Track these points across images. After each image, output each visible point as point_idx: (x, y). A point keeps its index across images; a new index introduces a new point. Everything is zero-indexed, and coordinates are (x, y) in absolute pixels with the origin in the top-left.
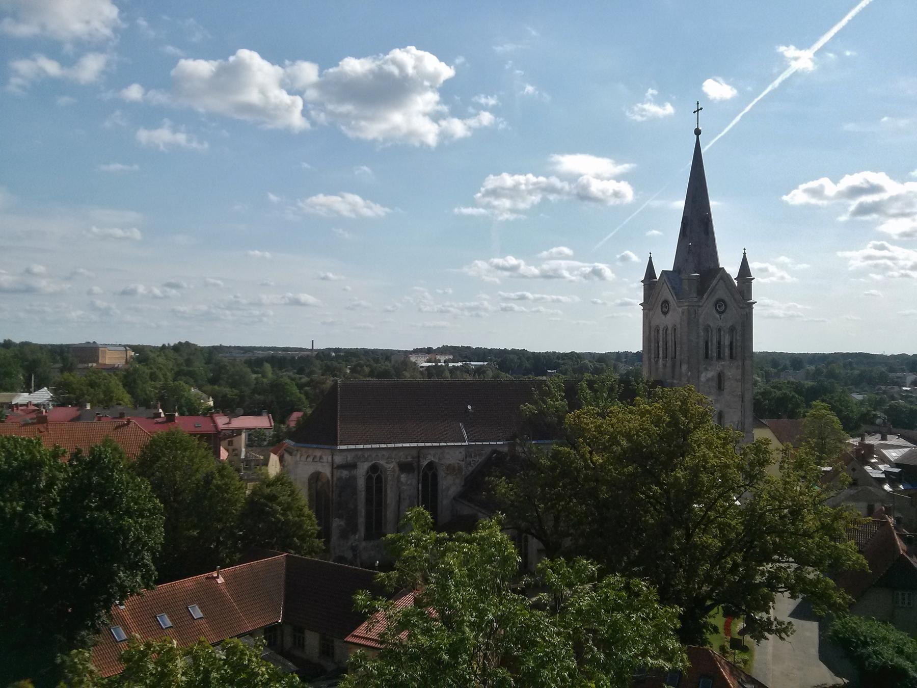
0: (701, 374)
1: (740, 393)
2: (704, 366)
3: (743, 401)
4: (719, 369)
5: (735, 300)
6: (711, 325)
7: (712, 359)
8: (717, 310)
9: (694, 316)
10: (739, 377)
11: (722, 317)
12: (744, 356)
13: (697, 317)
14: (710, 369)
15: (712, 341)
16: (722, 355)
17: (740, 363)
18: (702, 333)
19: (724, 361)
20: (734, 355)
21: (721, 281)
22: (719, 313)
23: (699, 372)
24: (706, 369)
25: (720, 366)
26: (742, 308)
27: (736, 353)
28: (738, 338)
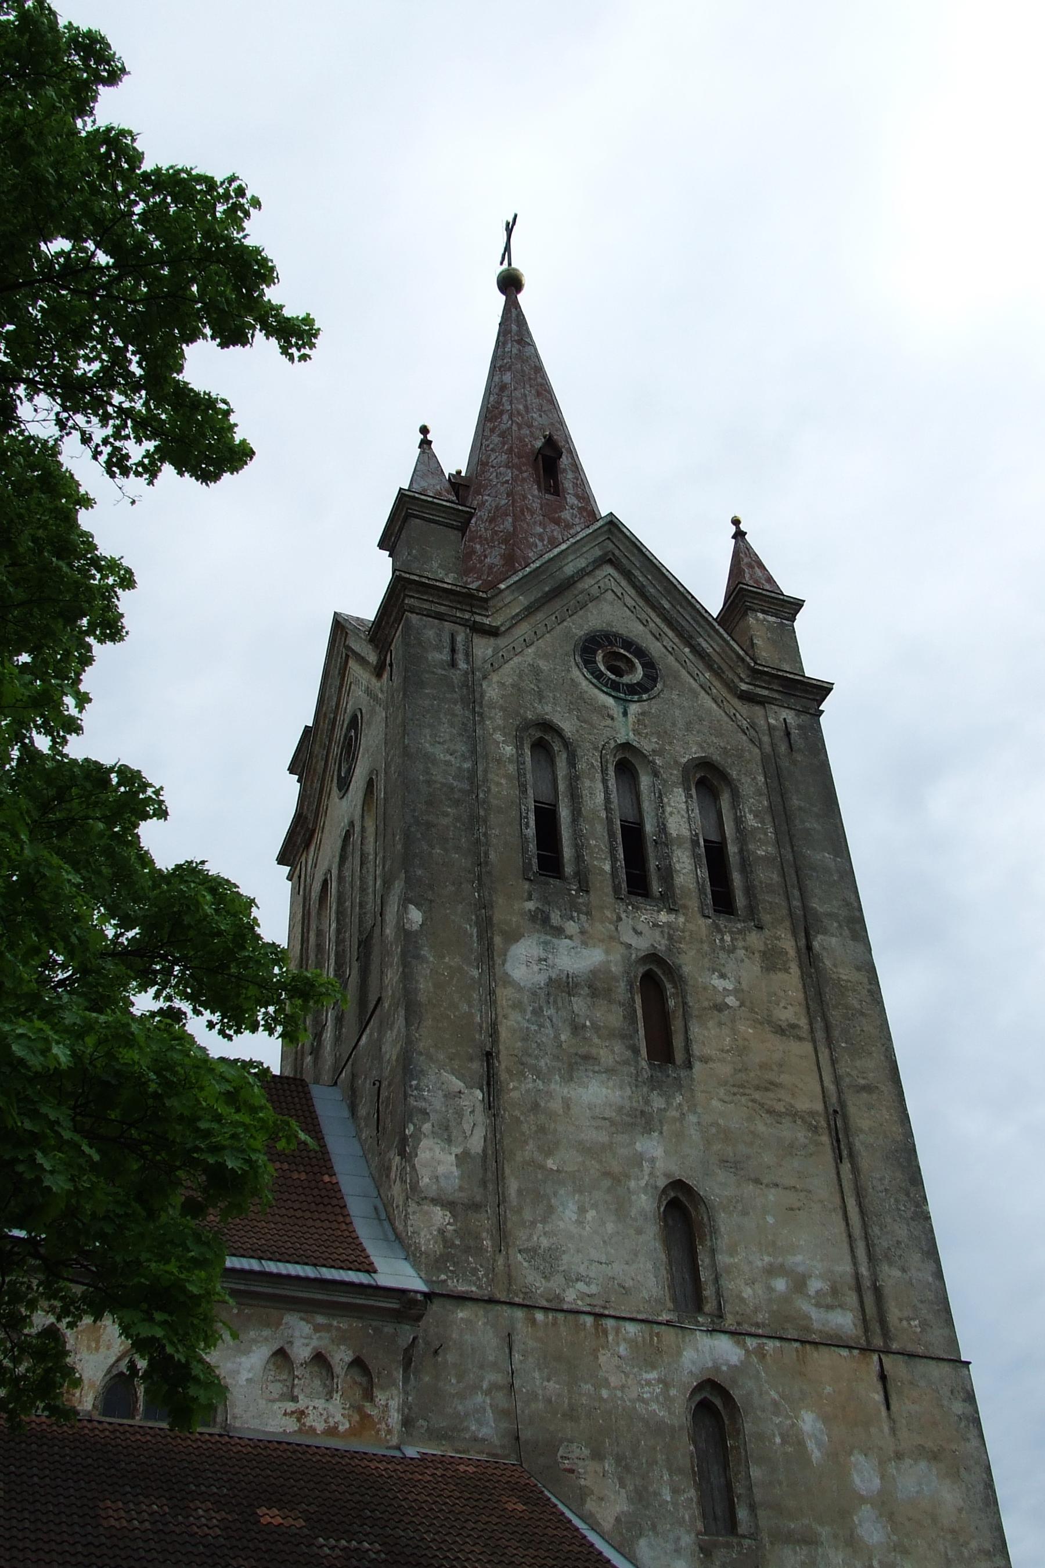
0: (513, 937)
1: (819, 1107)
2: (531, 905)
4: (642, 945)
5: (699, 653)
6: (568, 726)
7: (584, 887)
8: (599, 675)
9: (445, 656)
10: (790, 1013)
11: (634, 708)
12: (805, 907)
13: (463, 665)
14: (571, 927)
15: (575, 797)
16: (656, 888)
17: (788, 945)
18: (509, 750)
19: (671, 910)
20: (740, 900)
21: (609, 570)
22: (615, 686)
23: (486, 926)
24: (541, 920)
25: (640, 927)
26: (746, 697)
27: (749, 891)
28: (751, 820)
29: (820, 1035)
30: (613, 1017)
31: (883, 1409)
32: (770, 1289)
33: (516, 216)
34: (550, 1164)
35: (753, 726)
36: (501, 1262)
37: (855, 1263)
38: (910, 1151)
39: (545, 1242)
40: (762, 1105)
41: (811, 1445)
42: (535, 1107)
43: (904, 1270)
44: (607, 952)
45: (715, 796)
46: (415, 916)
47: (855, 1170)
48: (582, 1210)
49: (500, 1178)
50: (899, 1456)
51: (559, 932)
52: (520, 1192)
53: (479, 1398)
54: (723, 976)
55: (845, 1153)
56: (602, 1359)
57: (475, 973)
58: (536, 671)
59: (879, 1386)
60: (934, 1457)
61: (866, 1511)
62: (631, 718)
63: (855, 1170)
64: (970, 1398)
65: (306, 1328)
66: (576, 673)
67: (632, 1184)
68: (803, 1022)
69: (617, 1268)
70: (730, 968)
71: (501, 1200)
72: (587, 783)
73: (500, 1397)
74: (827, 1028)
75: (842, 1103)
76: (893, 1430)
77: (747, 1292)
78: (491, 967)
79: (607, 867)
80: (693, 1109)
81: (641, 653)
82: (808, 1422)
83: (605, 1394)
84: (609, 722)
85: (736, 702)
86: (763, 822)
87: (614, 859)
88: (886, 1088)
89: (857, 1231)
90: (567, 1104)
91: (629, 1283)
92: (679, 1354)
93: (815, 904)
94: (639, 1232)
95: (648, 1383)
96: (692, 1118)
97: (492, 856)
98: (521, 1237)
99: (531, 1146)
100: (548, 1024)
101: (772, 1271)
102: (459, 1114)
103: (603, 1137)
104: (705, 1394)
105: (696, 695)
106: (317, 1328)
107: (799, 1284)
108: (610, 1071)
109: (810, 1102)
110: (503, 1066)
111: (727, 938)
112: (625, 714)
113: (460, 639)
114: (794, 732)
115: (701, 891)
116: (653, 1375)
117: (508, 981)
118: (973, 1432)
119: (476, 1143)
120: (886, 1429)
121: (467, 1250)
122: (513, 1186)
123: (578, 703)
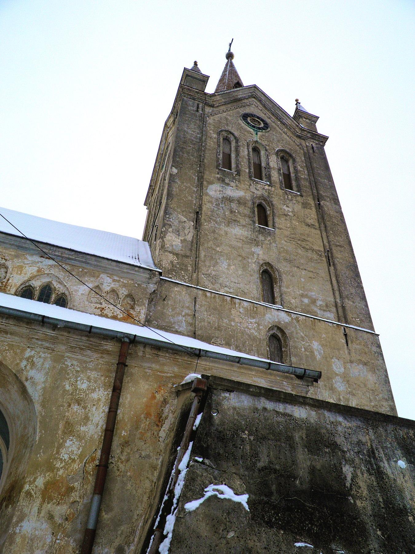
1: (322, 249)
3: (330, 260)
8: (248, 123)
9: (195, 109)
11: (259, 133)
12: (318, 193)
13: (201, 112)
14: (232, 184)
23: (201, 179)
29: (323, 228)
30: (247, 211)
31: (345, 345)
32: (302, 301)
33: (233, 39)
34: (218, 249)
35: (301, 144)
36: (195, 275)
37: (335, 298)
38: (356, 267)
39: (213, 273)
40: (301, 246)
41: (316, 353)
42: (214, 232)
43: (353, 302)
44: (245, 193)
45: (287, 161)
46: (175, 171)
47: (335, 269)
48: (229, 265)
49: (197, 249)
50: (351, 362)
51: (228, 184)
52: (205, 256)
53: (180, 318)
54: (287, 206)
55: (331, 264)
56: (233, 312)
57: (195, 190)
58: (227, 119)
59: (344, 337)
60: (365, 364)
61: (338, 378)
62: (258, 136)
63: (335, 269)
64: (379, 346)
65: (110, 280)
66: (240, 121)
67: (250, 260)
68: (317, 224)
69: (241, 285)
70: (290, 205)
71: (197, 257)
72: (242, 148)
73: (190, 319)
74: (326, 227)
75: (331, 249)
76: (349, 353)
77: (293, 301)
78: (202, 189)
79: (247, 171)
80: (275, 242)
81: (262, 120)
82: (315, 345)
83: (233, 324)
84: (251, 135)
85: (295, 137)
86: (304, 169)
87: (250, 169)
88: (347, 247)
89: (336, 288)
90: (226, 233)
91: (246, 291)
92: (264, 315)
93: (321, 192)
94: (251, 276)
95: (251, 323)
96: (274, 244)
97: (205, 161)
98: (204, 270)
99: (211, 242)
100: (221, 208)
101: (302, 296)
102: (184, 228)
103: (240, 245)
104: (275, 331)
105: (282, 134)
106: (114, 281)
107: (314, 302)
108: (244, 226)
109: (318, 246)
110: (203, 218)
111: (290, 197)
112: (257, 134)
113: (200, 106)
114: (315, 148)
115: (281, 182)
116: (254, 320)
117: (207, 194)
118: (380, 358)
119: (189, 237)
120: (346, 352)
121: (182, 269)
122: (202, 254)
123: (240, 128)
